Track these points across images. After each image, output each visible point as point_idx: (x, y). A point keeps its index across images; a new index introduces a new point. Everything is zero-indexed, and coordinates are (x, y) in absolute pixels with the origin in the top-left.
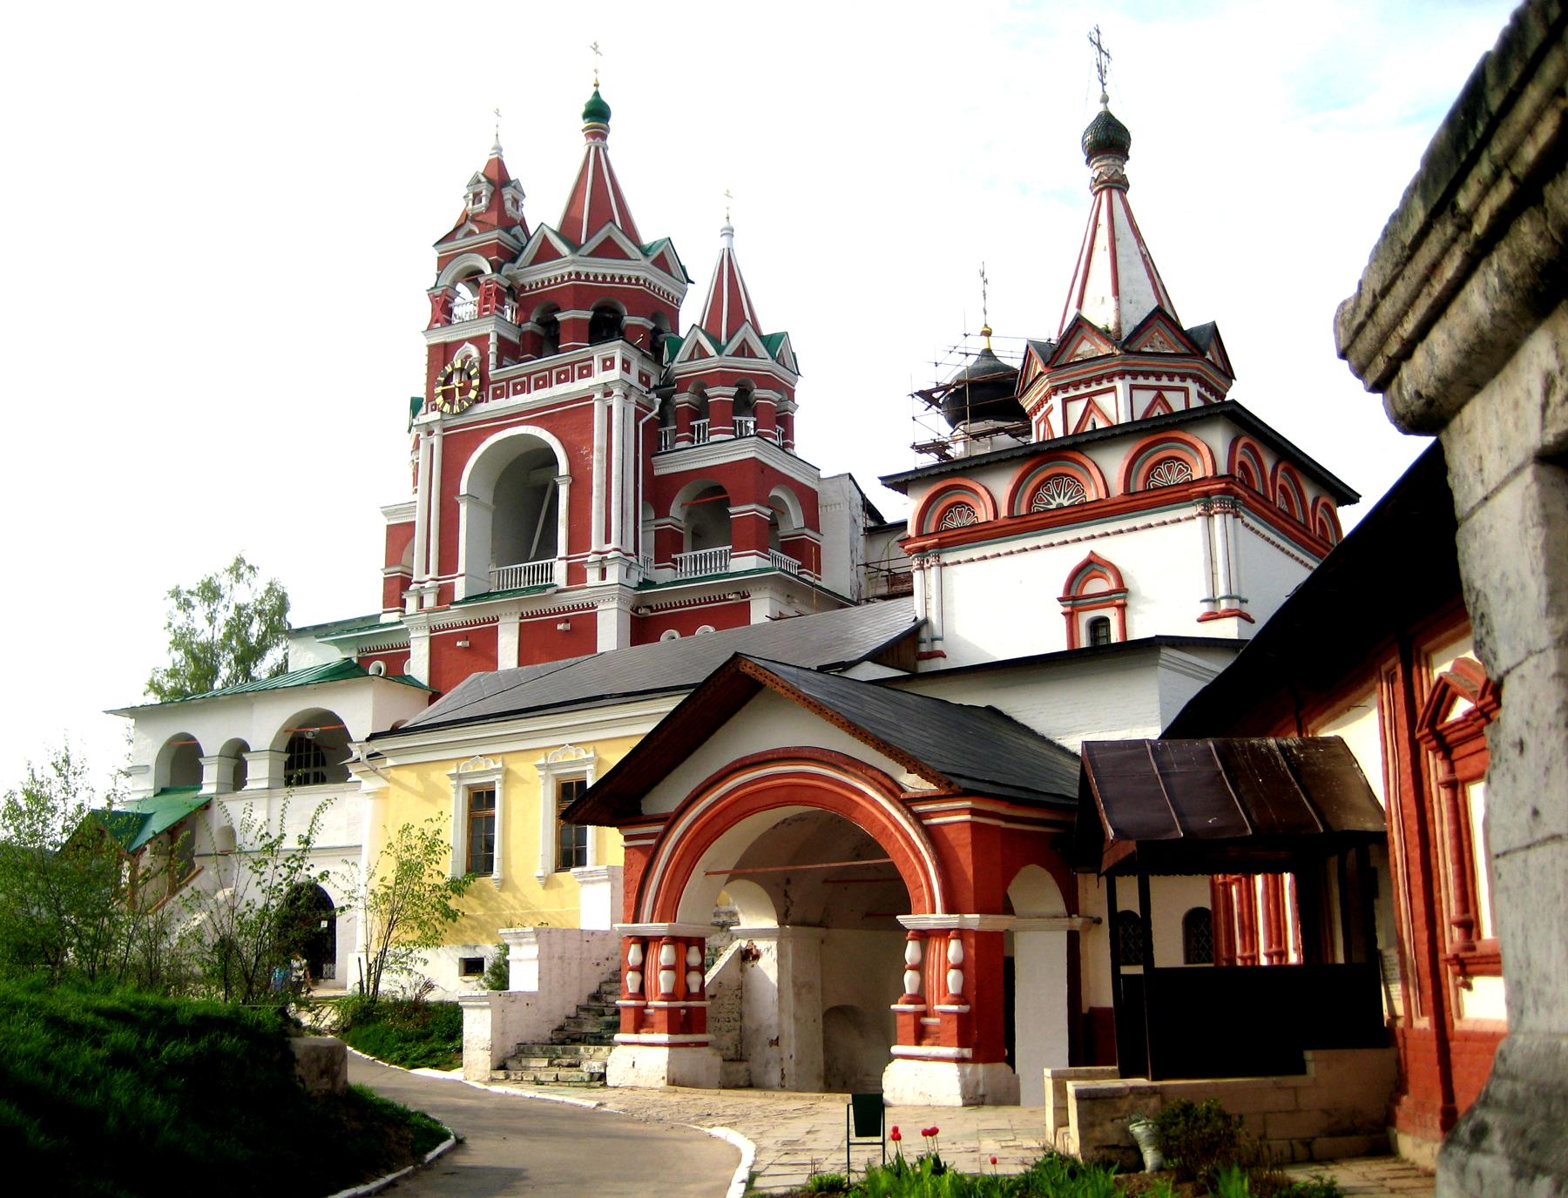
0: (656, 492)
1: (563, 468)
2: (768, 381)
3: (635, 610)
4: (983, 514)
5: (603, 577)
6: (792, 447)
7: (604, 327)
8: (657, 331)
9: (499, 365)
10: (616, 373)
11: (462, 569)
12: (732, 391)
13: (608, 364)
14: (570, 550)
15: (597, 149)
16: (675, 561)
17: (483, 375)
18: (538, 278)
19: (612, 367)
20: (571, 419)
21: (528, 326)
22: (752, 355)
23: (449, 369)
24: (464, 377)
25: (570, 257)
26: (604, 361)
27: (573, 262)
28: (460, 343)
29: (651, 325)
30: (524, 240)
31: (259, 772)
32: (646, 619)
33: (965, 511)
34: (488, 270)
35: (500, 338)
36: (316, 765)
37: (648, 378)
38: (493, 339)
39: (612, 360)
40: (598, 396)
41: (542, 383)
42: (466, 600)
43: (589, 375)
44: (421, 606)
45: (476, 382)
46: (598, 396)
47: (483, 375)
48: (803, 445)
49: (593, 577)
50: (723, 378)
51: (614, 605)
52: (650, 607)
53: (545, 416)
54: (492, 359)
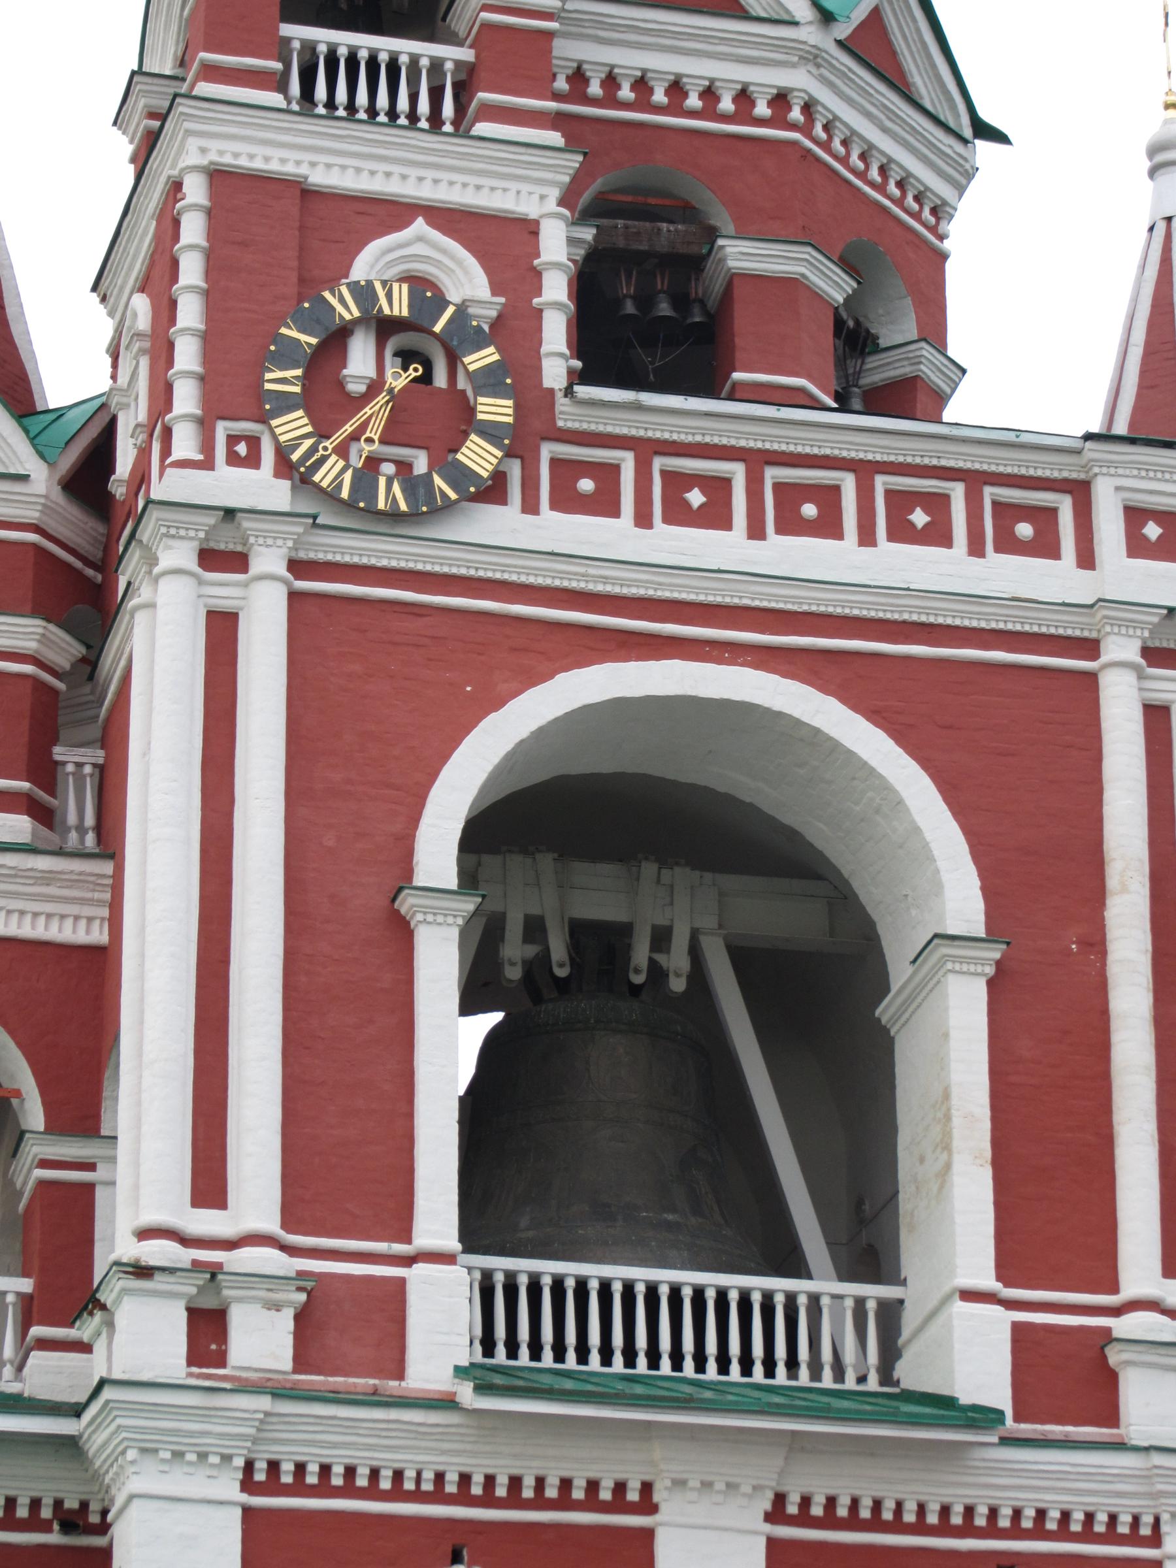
14: (1017, 1257)
17: (518, 375)
18: (629, 61)
25: (810, 34)
27: (813, 58)
28: (392, 213)
38: (557, 246)
40: (1122, 648)
41: (805, 510)
43: (1045, 546)
54: (555, 333)
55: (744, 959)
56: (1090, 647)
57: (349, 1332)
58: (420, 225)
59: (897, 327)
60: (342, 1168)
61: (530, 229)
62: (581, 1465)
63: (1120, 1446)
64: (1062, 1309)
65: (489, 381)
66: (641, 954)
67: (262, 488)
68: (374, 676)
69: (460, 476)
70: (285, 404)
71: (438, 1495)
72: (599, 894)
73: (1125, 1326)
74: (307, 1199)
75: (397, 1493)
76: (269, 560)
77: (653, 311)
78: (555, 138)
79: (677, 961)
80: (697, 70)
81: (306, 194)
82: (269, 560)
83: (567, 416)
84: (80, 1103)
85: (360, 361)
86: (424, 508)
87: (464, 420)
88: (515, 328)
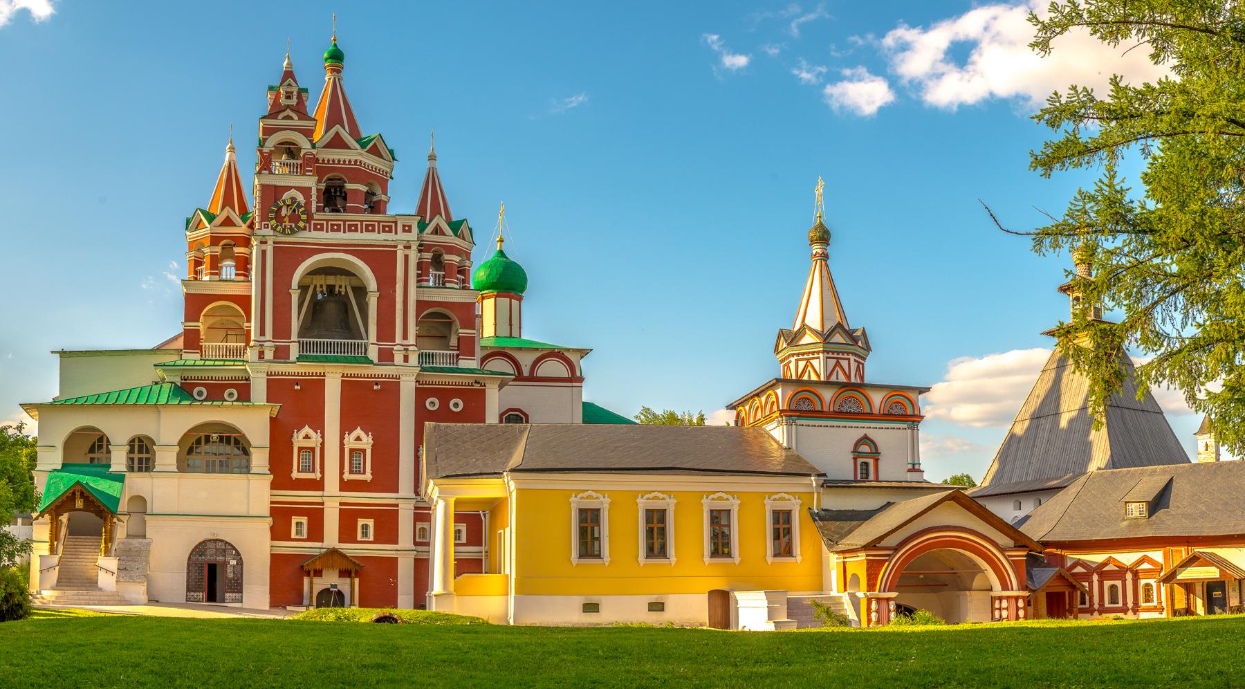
9: (319, 209)
11: (294, 337)
19: (410, 231)
20: (382, 260)
26: (404, 226)
28: (288, 188)
31: (166, 458)
36: (140, 451)
38: (314, 191)
39: (410, 227)
40: (400, 247)
41: (353, 228)
43: (390, 231)
46: (400, 247)
49: (398, 358)
50: (451, 250)
55: (353, 288)
57: (281, 354)
59: (378, 191)
60: (281, 330)
61: (310, 188)
62: (314, 370)
64: (386, 345)
65: (303, 213)
66: (337, 289)
67: (269, 232)
68: (286, 258)
69: (299, 228)
72: (331, 280)
74: (276, 335)
76: (270, 242)
77: (333, 196)
79: (343, 290)
80: (342, 158)
82: (270, 242)
83: (315, 217)
84: (249, 321)
85: (284, 212)
86: (293, 232)
87: (299, 219)
88: (308, 204)
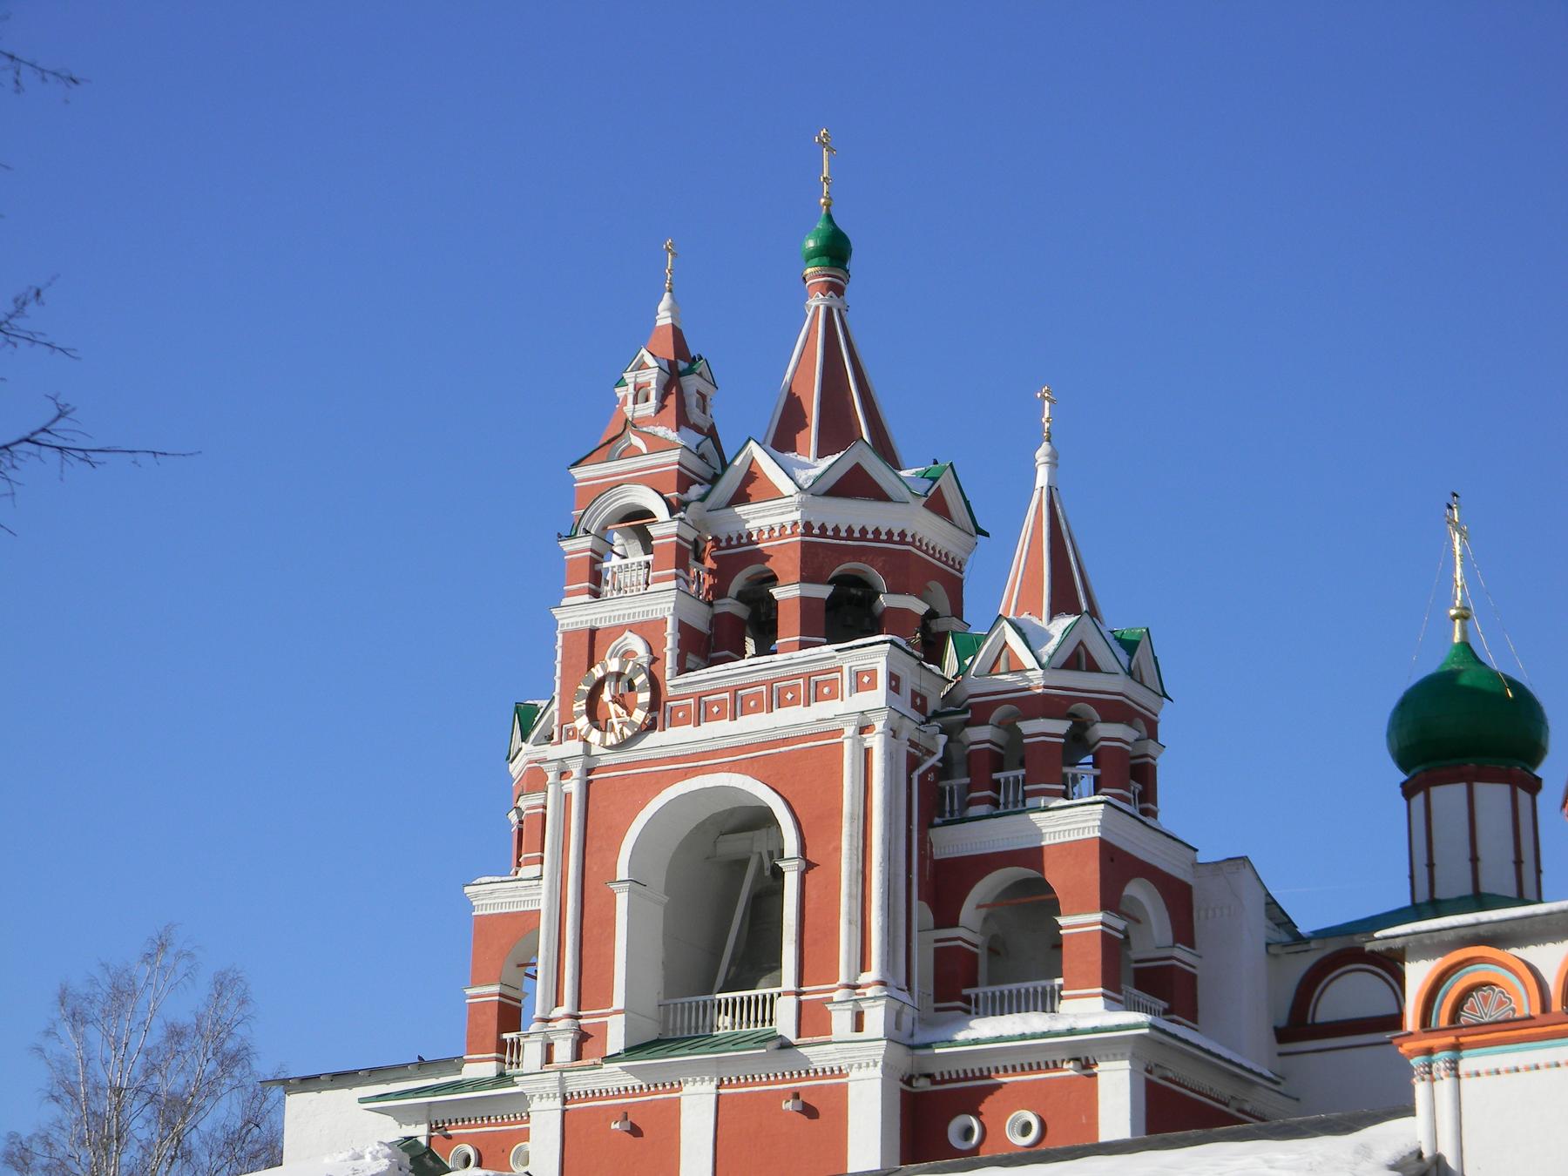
0: (937, 884)
1: (791, 845)
2: (1116, 710)
3: (908, 1080)
4: (1525, 1003)
5: (859, 1026)
6: (1154, 815)
7: (845, 614)
8: (932, 614)
9: (682, 669)
10: (877, 697)
11: (619, 1001)
12: (1062, 726)
13: (863, 681)
15: (829, 311)
16: (967, 999)
19: (873, 685)
20: (805, 769)
21: (729, 605)
22: (1093, 667)
23: (598, 672)
24: (622, 687)
29: (919, 607)
30: (717, 464)
32: (925, 1095)
33: (1494, 996)
34: (661, 512)
35: (683, 628)
37: (924, 699)
39: (873, 673)
42: (632, 1050)
43: (833, 696)
44: (548, 1059)
45: (644, 697)
46: (850, 730)
47: (655, 685)
48: (1169, 814)
49: (841, 1021)
51: (877, 1072)
52: (929, 1076)
53: (762, 760)
56: (840, 732)
58: (627, 634)
63: (830, 1042)
70: (580, 715)
71: (619, 1096)
73: (837, 996)
75: (608, 1097)
78: (673, 584)
81: (593, 632)
